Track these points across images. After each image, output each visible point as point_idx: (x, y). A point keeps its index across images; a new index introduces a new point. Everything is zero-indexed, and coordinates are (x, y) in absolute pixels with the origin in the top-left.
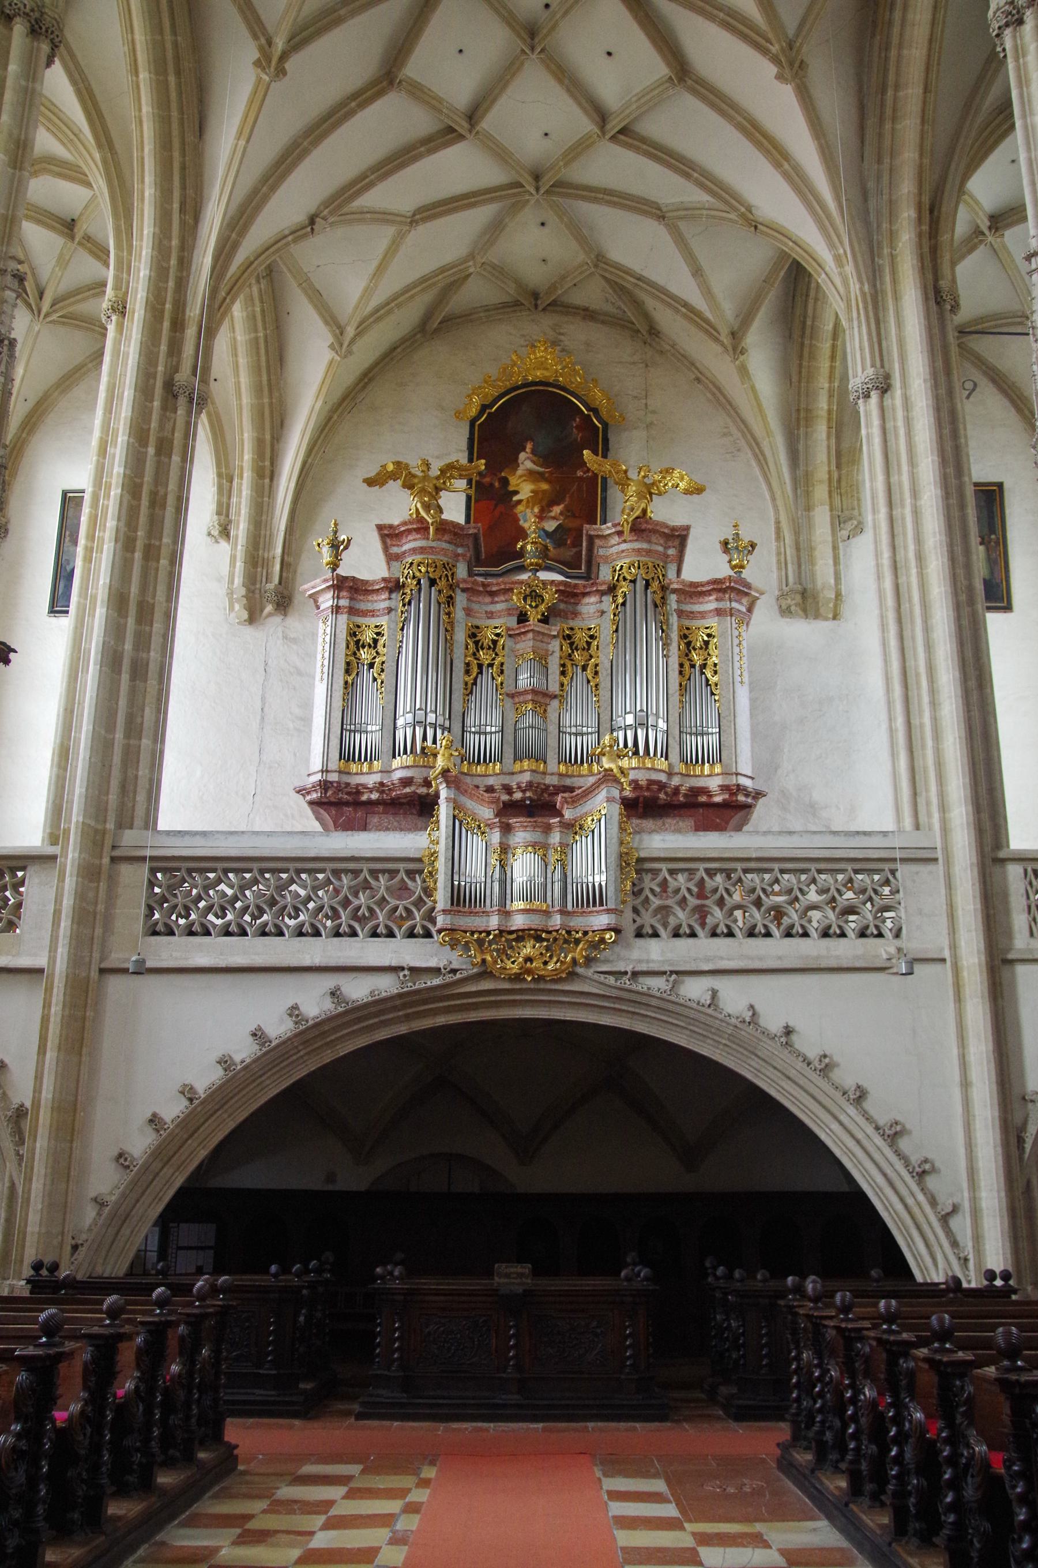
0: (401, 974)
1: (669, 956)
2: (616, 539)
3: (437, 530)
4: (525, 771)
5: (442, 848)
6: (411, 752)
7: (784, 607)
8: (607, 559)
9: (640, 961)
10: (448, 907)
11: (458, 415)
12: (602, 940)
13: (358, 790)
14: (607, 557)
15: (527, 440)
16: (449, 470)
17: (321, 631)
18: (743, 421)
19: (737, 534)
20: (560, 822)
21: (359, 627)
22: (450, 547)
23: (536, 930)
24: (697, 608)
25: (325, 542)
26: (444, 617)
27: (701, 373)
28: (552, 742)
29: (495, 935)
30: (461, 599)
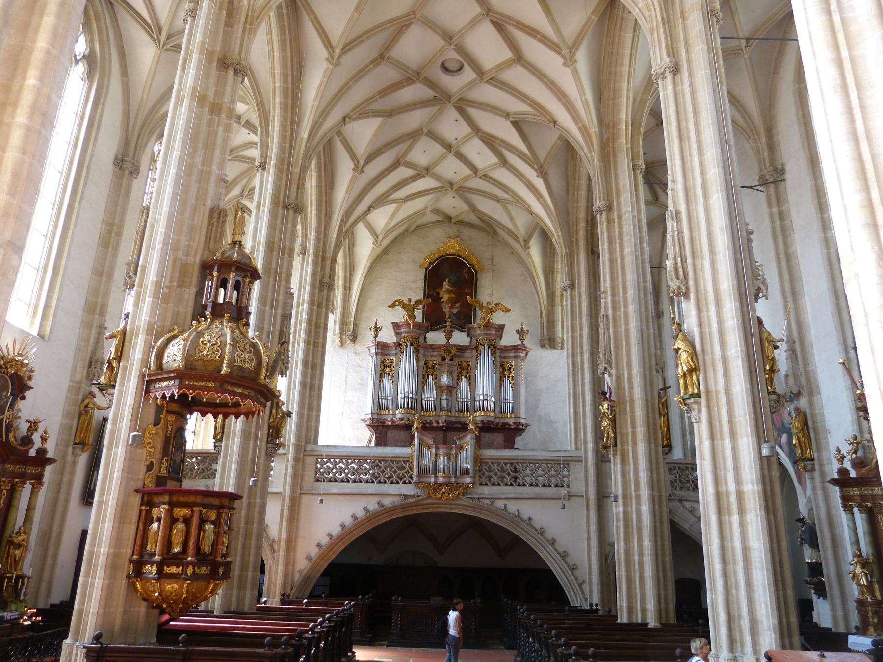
16: (417, 302)
28: (454, 405)
30: (421, 350)
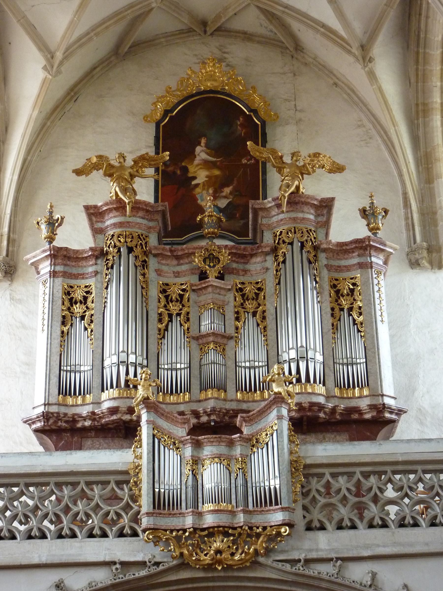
0: (114, 568)
1: (335, 545)
2: (275, 211)
3: (133, 208)
4: (209, 399)
5: (144, 462)
6: (117, 387)
7: (413, 261)
8: (270, 227)
9: (311, 550)
10: (151, 510)
11: (146, 118)
12: (279, 534)
13: (74, 419)
14: (269, 225)
15: (200, 137)
17: (41, 292)
18: (373, 116)
19: (372, 203)
20: (240, 437)
21: (72, 287)
22: (144, 222)
23: (224, 527)
24: (343, 263)
25: (43, 221)
26: (140, 277)
27: (337, 78)
28: (230, 375)
29: (190, 533)
30: (153, 263)
